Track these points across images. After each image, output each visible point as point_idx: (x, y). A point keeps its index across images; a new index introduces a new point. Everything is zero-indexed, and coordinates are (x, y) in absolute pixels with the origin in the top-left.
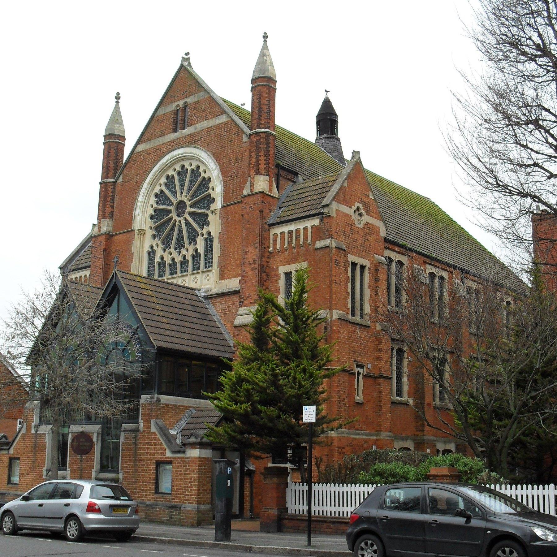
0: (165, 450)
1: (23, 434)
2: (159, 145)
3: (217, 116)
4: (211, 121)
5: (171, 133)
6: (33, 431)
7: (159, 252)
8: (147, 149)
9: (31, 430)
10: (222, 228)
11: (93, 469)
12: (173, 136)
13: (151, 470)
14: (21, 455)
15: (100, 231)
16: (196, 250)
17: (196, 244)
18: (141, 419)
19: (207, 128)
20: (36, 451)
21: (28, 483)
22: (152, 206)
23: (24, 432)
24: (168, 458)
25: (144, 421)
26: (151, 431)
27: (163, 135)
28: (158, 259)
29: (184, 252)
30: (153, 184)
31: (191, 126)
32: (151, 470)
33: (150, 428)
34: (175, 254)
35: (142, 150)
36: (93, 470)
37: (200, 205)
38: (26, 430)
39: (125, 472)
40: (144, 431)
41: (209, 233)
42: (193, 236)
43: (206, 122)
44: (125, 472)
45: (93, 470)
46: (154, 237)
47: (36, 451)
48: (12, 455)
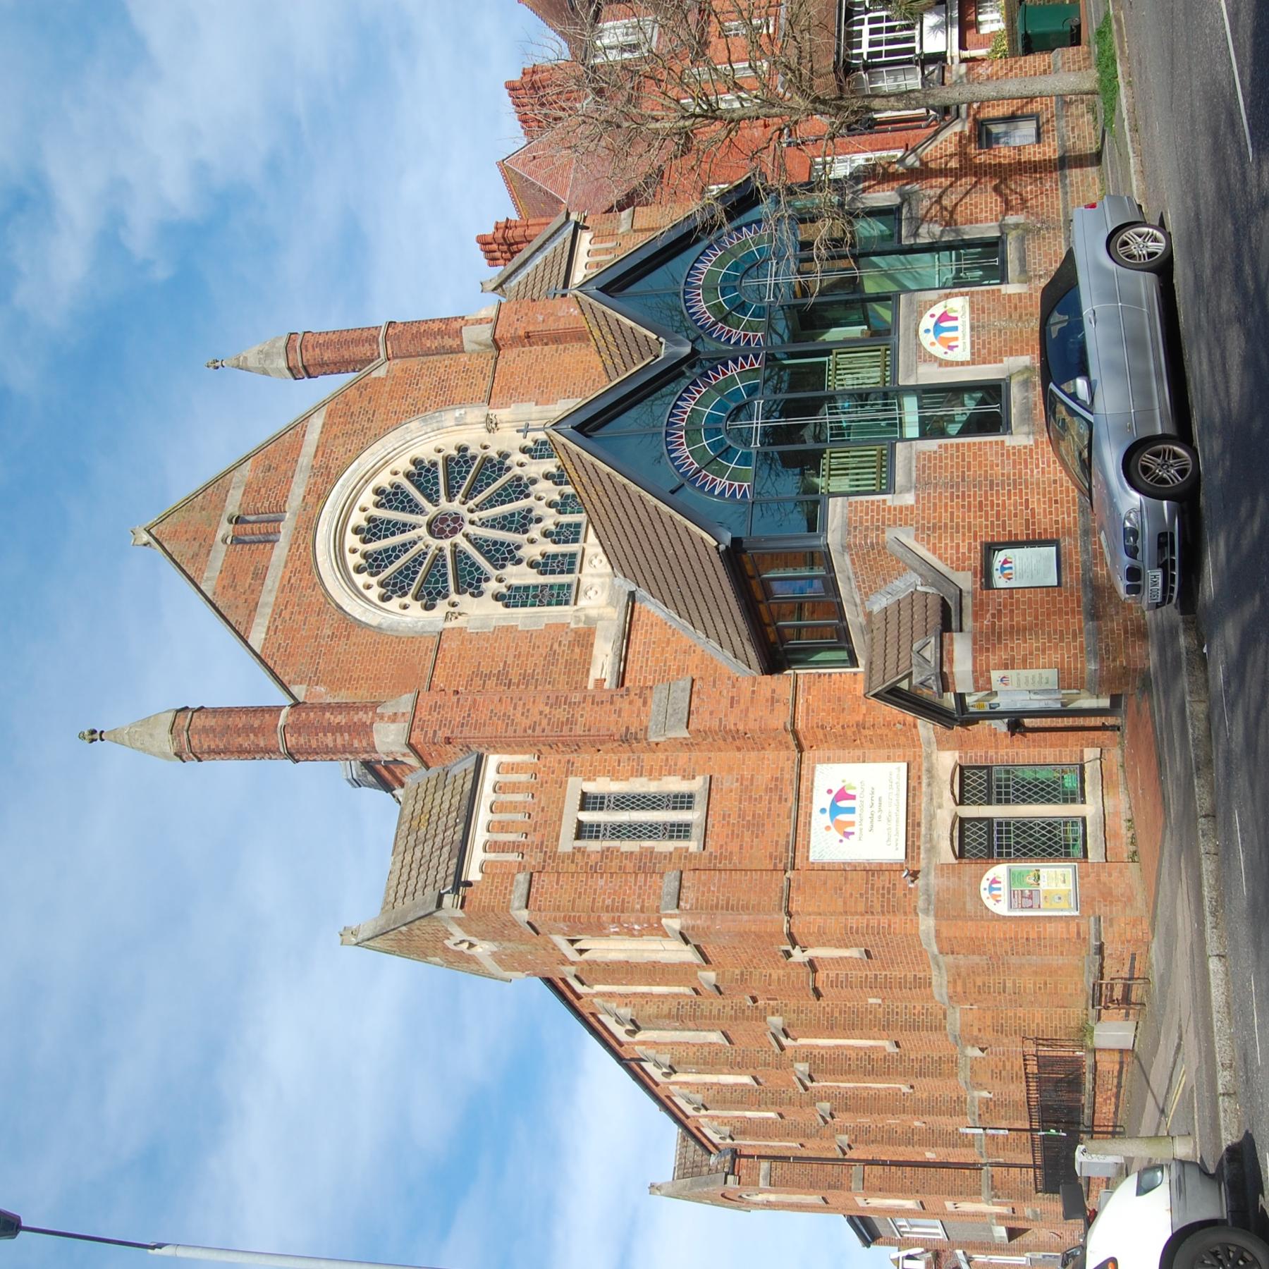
1: (916, 539)
3: (304, 436)
4: (304, 451)
5: (272, 548)
6: (909, 499)
8: (274, 610)
10: (530, 400)
15: (403, 714)
17: (533, 481)
19: (315, 457)
20: (963, 480)
22: (405, 607)
23: (912, 530)
27: (267, 568)
29: (540, 509)
31: (287, 497)
34: (535, 531)
35: (265, 630)
36: (1003, 292)
37: (457, 482)
38: (906, 524)
41: (524, 450)
42: (519, 488)
45: (1003, 292)
47: (963, 480)
48: (975, 576)
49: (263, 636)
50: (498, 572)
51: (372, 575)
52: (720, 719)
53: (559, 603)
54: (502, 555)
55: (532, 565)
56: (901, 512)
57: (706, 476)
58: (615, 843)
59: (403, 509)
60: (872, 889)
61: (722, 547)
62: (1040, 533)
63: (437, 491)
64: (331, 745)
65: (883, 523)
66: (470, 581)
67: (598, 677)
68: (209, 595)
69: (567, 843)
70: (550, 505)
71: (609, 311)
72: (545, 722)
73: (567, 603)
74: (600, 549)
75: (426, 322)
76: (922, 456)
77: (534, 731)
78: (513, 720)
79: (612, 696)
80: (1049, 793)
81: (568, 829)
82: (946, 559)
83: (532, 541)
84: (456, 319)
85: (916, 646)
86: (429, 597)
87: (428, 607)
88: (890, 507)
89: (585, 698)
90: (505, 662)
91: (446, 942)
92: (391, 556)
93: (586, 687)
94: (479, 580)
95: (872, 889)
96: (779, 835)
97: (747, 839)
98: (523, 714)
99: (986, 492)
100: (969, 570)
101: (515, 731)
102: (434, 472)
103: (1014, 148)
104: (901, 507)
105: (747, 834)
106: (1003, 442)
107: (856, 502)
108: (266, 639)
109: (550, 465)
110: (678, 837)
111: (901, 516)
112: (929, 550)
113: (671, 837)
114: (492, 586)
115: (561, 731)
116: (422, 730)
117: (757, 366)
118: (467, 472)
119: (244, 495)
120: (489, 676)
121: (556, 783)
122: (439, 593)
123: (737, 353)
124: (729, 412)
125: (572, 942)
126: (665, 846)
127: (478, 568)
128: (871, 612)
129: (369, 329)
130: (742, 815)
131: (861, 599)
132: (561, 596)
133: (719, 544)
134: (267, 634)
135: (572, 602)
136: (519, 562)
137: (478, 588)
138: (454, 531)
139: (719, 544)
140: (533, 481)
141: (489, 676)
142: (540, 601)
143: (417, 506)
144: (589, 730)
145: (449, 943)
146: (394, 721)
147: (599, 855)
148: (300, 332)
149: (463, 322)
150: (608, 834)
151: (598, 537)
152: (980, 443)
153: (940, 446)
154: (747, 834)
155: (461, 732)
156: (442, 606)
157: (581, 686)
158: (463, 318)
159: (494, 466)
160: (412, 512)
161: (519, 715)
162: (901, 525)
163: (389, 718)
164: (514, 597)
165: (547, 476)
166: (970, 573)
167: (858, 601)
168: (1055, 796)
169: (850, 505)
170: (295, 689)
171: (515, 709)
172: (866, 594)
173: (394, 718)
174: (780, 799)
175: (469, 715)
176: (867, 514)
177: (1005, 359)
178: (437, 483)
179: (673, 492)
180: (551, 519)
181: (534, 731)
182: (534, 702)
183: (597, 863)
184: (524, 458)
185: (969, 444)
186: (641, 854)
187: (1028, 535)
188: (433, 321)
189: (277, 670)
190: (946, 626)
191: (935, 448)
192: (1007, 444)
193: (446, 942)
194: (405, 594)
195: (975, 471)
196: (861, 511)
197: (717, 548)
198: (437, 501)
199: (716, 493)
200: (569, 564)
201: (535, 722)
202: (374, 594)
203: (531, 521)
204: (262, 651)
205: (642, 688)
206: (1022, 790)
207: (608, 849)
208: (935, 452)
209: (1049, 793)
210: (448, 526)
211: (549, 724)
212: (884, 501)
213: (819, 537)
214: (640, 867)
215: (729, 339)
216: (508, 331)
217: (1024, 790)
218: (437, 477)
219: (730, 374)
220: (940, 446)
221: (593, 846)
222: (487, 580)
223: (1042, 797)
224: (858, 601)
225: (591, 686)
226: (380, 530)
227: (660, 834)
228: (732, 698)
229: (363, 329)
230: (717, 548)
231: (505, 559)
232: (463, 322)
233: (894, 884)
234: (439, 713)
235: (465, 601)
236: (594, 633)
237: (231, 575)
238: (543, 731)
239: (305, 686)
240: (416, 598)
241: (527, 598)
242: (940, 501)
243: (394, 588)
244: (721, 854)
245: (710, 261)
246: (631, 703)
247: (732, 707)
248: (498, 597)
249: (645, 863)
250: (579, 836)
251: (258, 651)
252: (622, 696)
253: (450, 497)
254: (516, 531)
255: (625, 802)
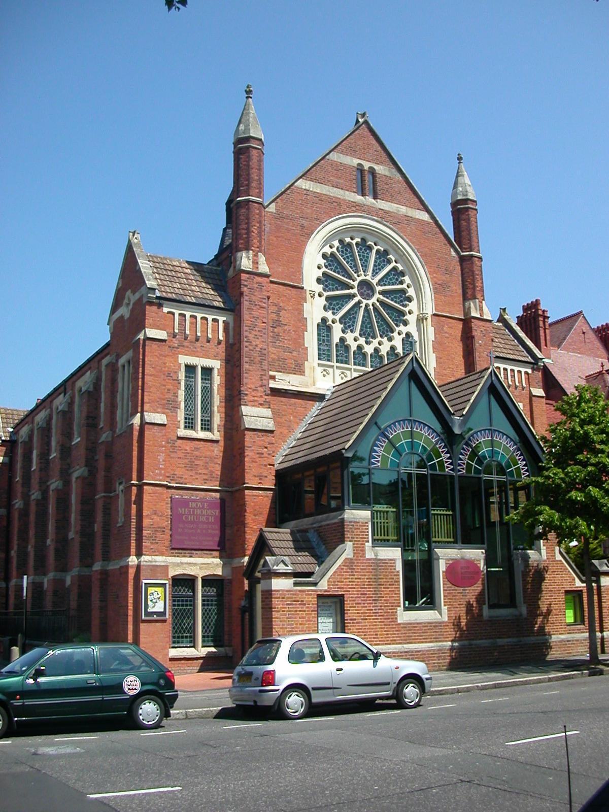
0: (574, 579)
1: (346, 559)
2: (337, 198)
4: (410, 209)
6: (369, 554)
7: (337, 332)
9: (364, 554)
11: (485, 604)
12: (359, 198)
13: (561, 601)
14: (344, 591)
15: (257, 268)
16: (393, 348)
18: (544, 545)
21: (367, 632)
23: (351, 556)
24: (577, 587)
25: (547, 548)
26: (557, 559)
28: (336, 340)
29: (375, 343)
30: (327, 241)
32: (561, 601)
33: (555, 556)
34: (362, 341)
35: (307, 188)
38: (354, 553)
39: (530, 605)
40: (547, 559)
42: (387, 331)
43: (404, 208)
44: (530, 605)
46: (325, 309)
48: (326, 591)
49: (304, 187)
50: (338, 320)
51: (338, 248)
52: (251, 447)
53: (319, 354)
54: (348, 321)
55: (342, 340)
56: (362, 551)
57: (385, 442)
58: (183, 387)
59: (375, 266)
60: (155, 531)
61: (344, 451)
62: (348, 626)
63: (385, 285)
64: (241, 227)
65: (355, 541)
66: (333, 303)
67: (277, 377)
68: (327, 157)
69: (184, 360)
70: (376, 350)
71: (479, 387)
72: (251, 348)
73: (319, 359)
74: (349, 379)
75: (482, 279)
76: (393, 562)
77: (246, 342)
78: (253, 330)
79: (265, 386)
80: (208, 628)
81: (192, 360)
82: (334, 575)
83: (355, 340)
84: (483, 296)
85: (286, 559)
86: (325, 280)
87: (319, 281)
88: (364, 544)
89: (264, 370)
90: (286, 325)
91: (130, 291)
92: (349, 259)
93: (271, 370)
94: (333, 309)
95: (155, 531)
96: (186, 479)
97: (184, 461)
98: (256, 335)
99: (372, 597)
100: (328, 588)
101: (246, 331)
102: (396, 283)
103: (565, 612)
104: (365, 551)
105: (187, 461)
106: (400, 606)
107: (368, 526)
108: (302, 189)
109: (400, 350)
110: (186, 423)
111: (359, 551)
112: (340, 566)
113: (186, 418)
114: (329, 315)
115: (246, 357)
116: (248, 278)
117: (446, 470)
118: (395, 302)
119: (385, 176)
120: (278, 315)
121: (217, 354)
122: (326, 286)
123: (454, 459)
124: (421, 455)
125: (129, 362)
126: (181, 415)
127: (340, 308)
128: (308, 532)
129: (478, 246)
130: (197, 458)
131: (315, 527)
132: (324, 355)
133: (346, 450)
134: (305, 190)
135: (320, 362)
136: (343, 332)
137: (329, 308)
138: (361, 295)
139: (346, 450)
140: (390, 339)
141: (278, 315)
142: (321, 344)
143: (377, 273)
144: (246, 373)
145: (129, 293)
146: (253, 262)
147: (176, 378)
148: (477, 208)
149: (481, 300)
150: (188, 383)
151: (355, 378)
152: (399, 594)
153: (398, 572)
154: (187, 461)
155: (246, 300)
156: (319, 288)
157: (272, 367)
158: (484, 300)
159: (400, 317)
160: (373, 270)
161: (255, 333)
162: (354, 550)
163: (255, 260)
164: (324, 327)
165: (393, 348)
166: (326, 588)
167: (314, 526)
168: (206, 631)
169: (367, 523)
170: (273, 205)
171: (259, 331)
172: (317, 530)
173: (255, 263)
174: (206, 480)
175: (256, 305)
176: (361, 532)
177: (446, 607)
178: (389, 285)
179: (376, 423)
180: (369, 349)
181: (246, 342)
182: (263, 342)
183: (171, 377)
184: (403, 335)
185: (399, 588)
186: (177, 402)
187: (347, 620)
188: (482, 283)
189: (284, 196)
190: (296, 575)
191: (397, 569)
192: (398, 608)
193: (130, 291)
194: (326, 267)
195: (383, 591)
196: (362, 529)
197: (344, 449)
198: (380, 285)
199: (375, 448)
200: (343, 359)
201: (251, 342)
202: (328, 250)
203: (367, 338)
204: (295, 187)
205: (269, 402)
206: (210, 613)
207: (180, 383)
208: (395, 569)
209: (208, 628)
210: (365, 291)
211: (250, 350)
212: (368, 542)
213: (349, 505)
214: (169, 401)
215: (462, 454)
216: (475, 325)
217: (210, 613)
218: (393, 284)
219: (442, 455)
220: (398, 572)
221: (182, 375)
222: (333, 313)
223: (206, 624)
224: (314, 526)
225: (271, 373)
226: (363, 252)
227: (188, 413)
228: (263, 454)
229: (478, 243)
230: (344, 449)
231: (345, 324)
232: (481, 300)
233: (157, 543)
234: (257, 288)
235: (322, 301)
236: (301, 375)
237: (339, 168)
238: (246, 347)
239: (274, 211)
240: (324, 274)
241: (323, 336)
242: (368, 572)
243: (331, 259)
244: (176, 447)
245: (507, 443)
246: (261, 396)
247: (258, 453)
248: (324, 320)
249: (171, 404)
250: (187, 366)
251: (296, 184)
252: (265, 391)
253: (382, 293)
254: (361, 330)
255: (207, 392)
